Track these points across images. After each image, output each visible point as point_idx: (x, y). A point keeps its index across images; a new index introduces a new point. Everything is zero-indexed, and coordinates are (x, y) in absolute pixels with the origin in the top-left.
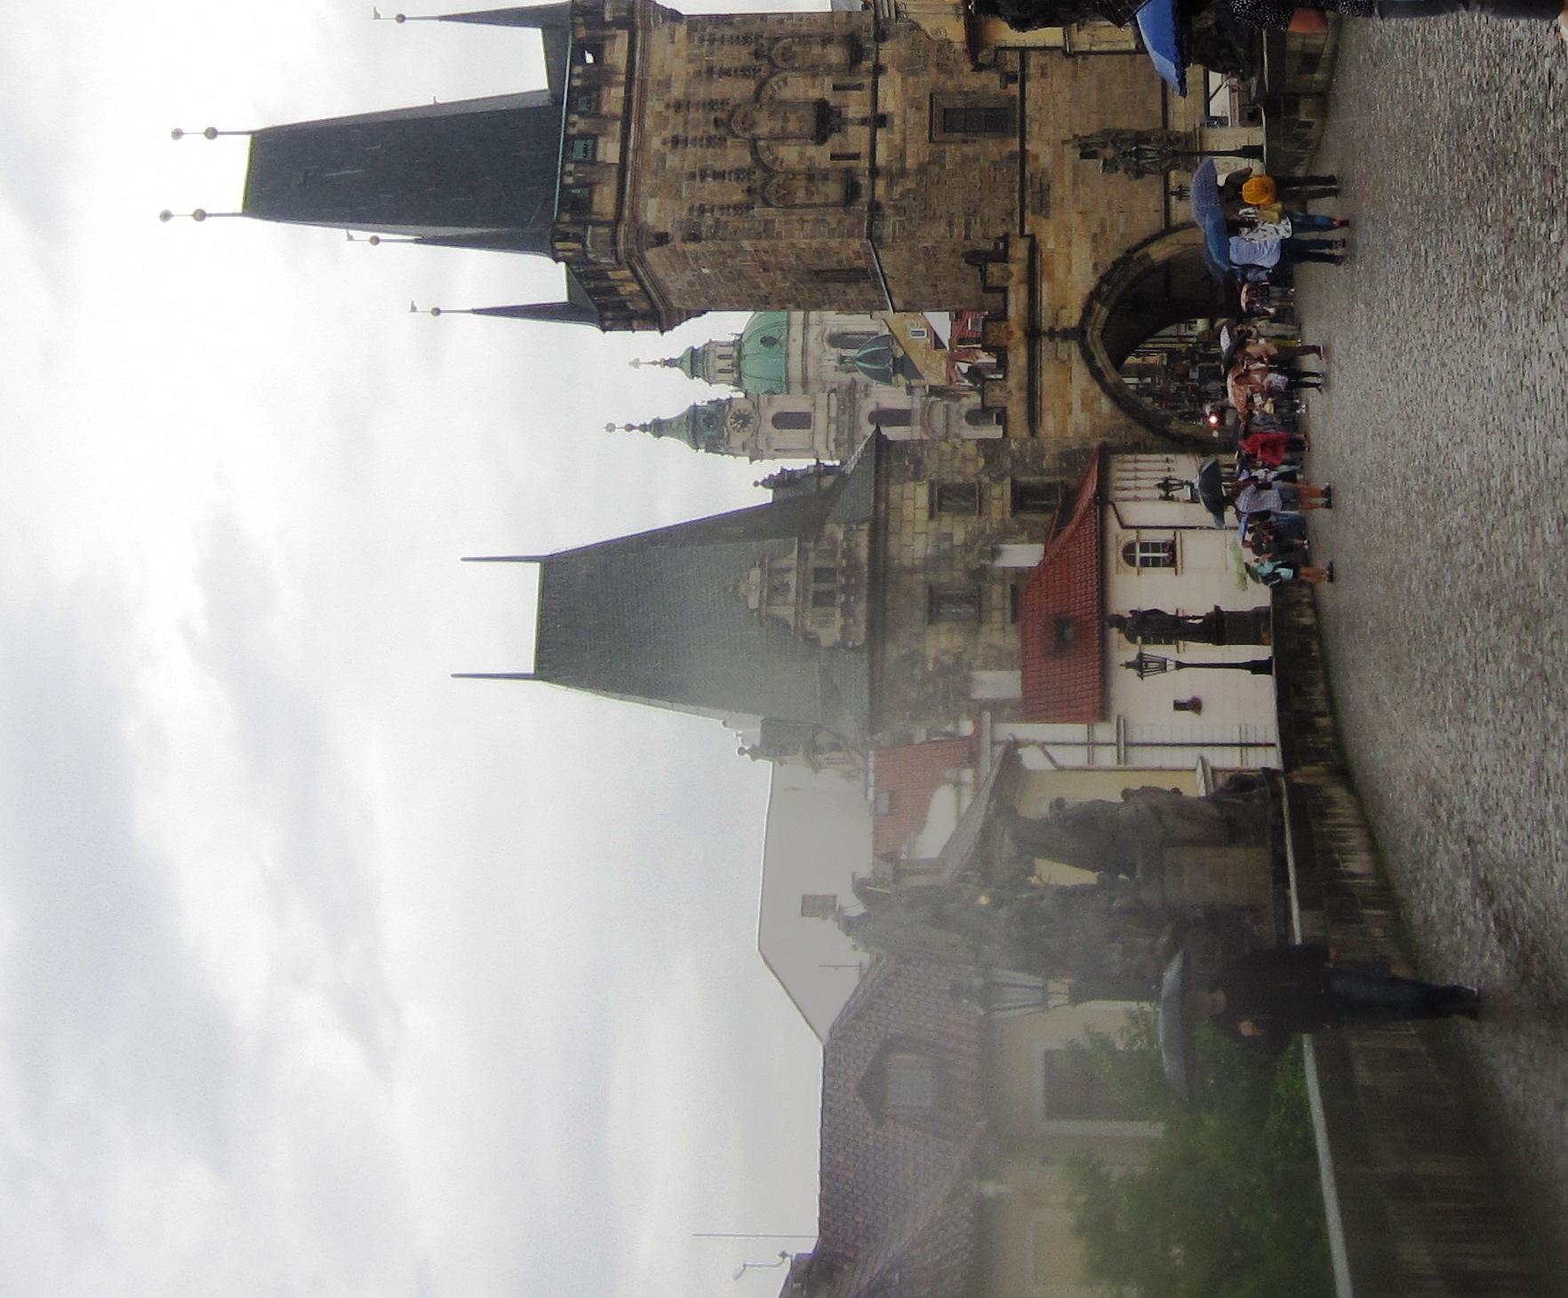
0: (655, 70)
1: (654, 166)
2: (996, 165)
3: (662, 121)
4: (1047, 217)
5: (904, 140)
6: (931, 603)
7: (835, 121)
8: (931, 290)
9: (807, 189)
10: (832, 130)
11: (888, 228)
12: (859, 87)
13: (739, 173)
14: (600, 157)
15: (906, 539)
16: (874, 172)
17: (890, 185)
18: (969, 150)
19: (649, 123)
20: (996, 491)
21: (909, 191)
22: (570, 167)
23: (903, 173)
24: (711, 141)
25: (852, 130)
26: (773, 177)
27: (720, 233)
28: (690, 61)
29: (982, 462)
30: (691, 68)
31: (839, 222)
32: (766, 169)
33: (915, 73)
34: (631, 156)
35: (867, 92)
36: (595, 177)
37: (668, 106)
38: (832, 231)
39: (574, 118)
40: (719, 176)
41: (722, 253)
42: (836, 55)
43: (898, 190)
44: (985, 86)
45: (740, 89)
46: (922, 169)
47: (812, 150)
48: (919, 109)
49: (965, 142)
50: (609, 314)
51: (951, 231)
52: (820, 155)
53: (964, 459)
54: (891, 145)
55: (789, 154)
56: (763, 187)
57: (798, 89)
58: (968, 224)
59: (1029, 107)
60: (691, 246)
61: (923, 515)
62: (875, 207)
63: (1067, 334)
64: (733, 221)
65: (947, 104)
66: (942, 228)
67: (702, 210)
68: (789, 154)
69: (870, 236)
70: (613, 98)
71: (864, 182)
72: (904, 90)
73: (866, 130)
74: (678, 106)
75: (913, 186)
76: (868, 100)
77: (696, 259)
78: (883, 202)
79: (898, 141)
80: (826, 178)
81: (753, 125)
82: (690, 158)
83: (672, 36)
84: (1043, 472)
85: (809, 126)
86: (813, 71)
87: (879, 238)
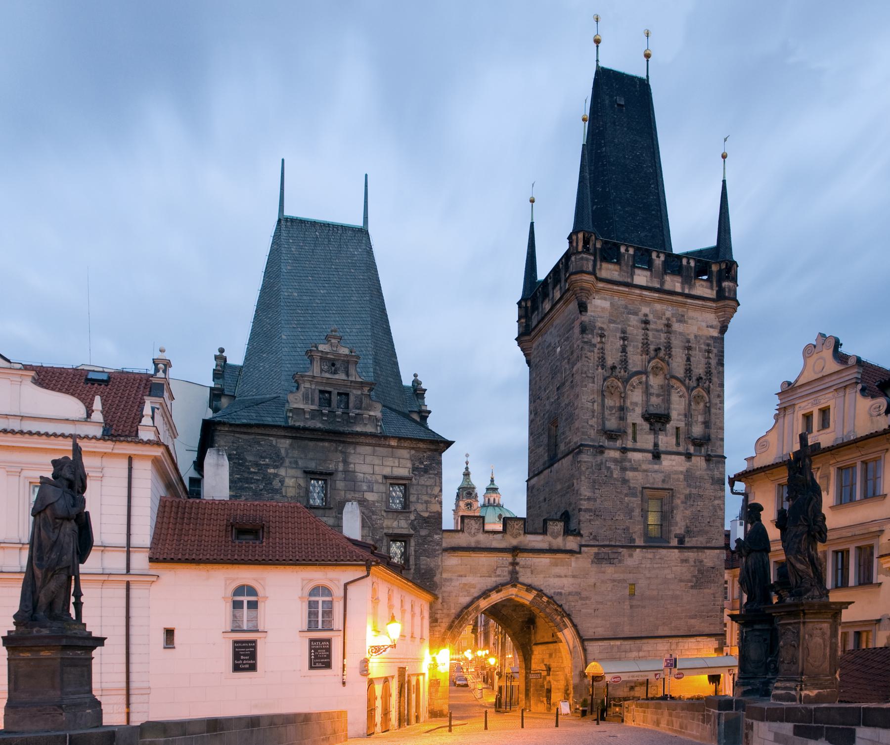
6: (321, 474)
7: (658, 426)
9: (614, 407)
10: (651, 424)
11: (586, 457)
12: (678, 444)
13: (624, 362)
15: (369, 459)
16: (624, 450)
17: (615, 461)
20: (403, 523)
21: (612, 473)
23: (624, 469)
24: (646, 344)
25: (651, 438)
26: (623, 383)
27: (586, 347)
31: (592, 426)
33: (686, 479)
35: (675, 449)
40: (624, 350)
41: (572, 353)
42: (697, 430)
45: (678, 366)
47: (639, 411)
48: (663, 481)
51: (585, 500)
53: (427, 502)
57: (678, 406)
60: (577, 330)
61: (387, 471)
62: (601, 450)
64: (594, 356)
67: (602, 336)
68: (636, 397)
69: (582, 445)
71: (618, 443)
72: (676, 473)
73: (650, 446)
75: (615, 476)
76: (669, 449)
77: (567, 339)
79: (644, 467)
82: (635, 332)
85: (652, 410)
86: (688, 415)
87: (580, 452)
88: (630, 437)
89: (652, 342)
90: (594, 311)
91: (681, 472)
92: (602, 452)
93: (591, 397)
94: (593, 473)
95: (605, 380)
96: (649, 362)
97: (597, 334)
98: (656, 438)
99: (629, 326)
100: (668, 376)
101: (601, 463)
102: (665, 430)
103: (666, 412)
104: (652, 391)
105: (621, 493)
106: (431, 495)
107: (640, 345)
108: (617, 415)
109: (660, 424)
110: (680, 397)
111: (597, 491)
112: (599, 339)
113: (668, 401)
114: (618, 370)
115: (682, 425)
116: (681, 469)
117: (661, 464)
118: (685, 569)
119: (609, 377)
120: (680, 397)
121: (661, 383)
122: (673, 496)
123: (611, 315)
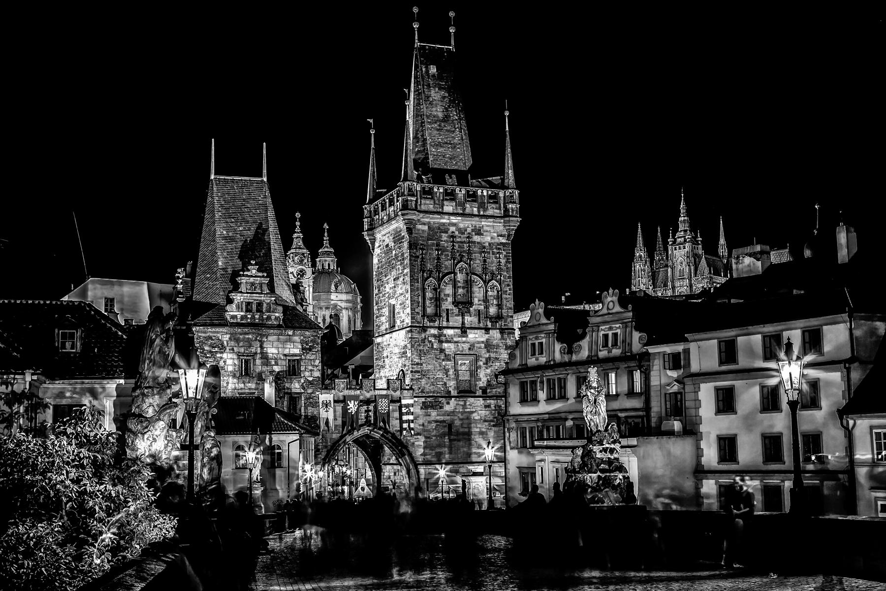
3: (462, 231)
4: (422, 408)
8: (385, 355)
17: (434, 336)
20: (297, 385)
23: (441, 342)
28: (490, 244)
29: (311, 379)
34: (447, 217)
42: (493, 310)
44: (480, 379)
46: (442, 351)
47: (450, 299)
48: (470, 349)
50: (372, 209)
52: (448, 304)
53: (311, 370)
54: (452, 337)
55: (449, 290)
58: (418, 372)
62: (424, 329)
63: (367, 417)
71: (436, 324)
72: (479, 343)
78: (428, 333)
79: (455, 339)
83: (501, 236)
84: (306, 408)
86: (486, 300)
87: (411, 331)
88: (445, 319)
91: (483, 342)
92: (425, 331)
94: (419, 345)
98: (463, 318)
102: (469, 312)
104: (459, 285)
106: (314, 366)
115: (482, 307)
116: (482, 340)
117: (467, 336)
118: (488, 413)
123: (429, 234)
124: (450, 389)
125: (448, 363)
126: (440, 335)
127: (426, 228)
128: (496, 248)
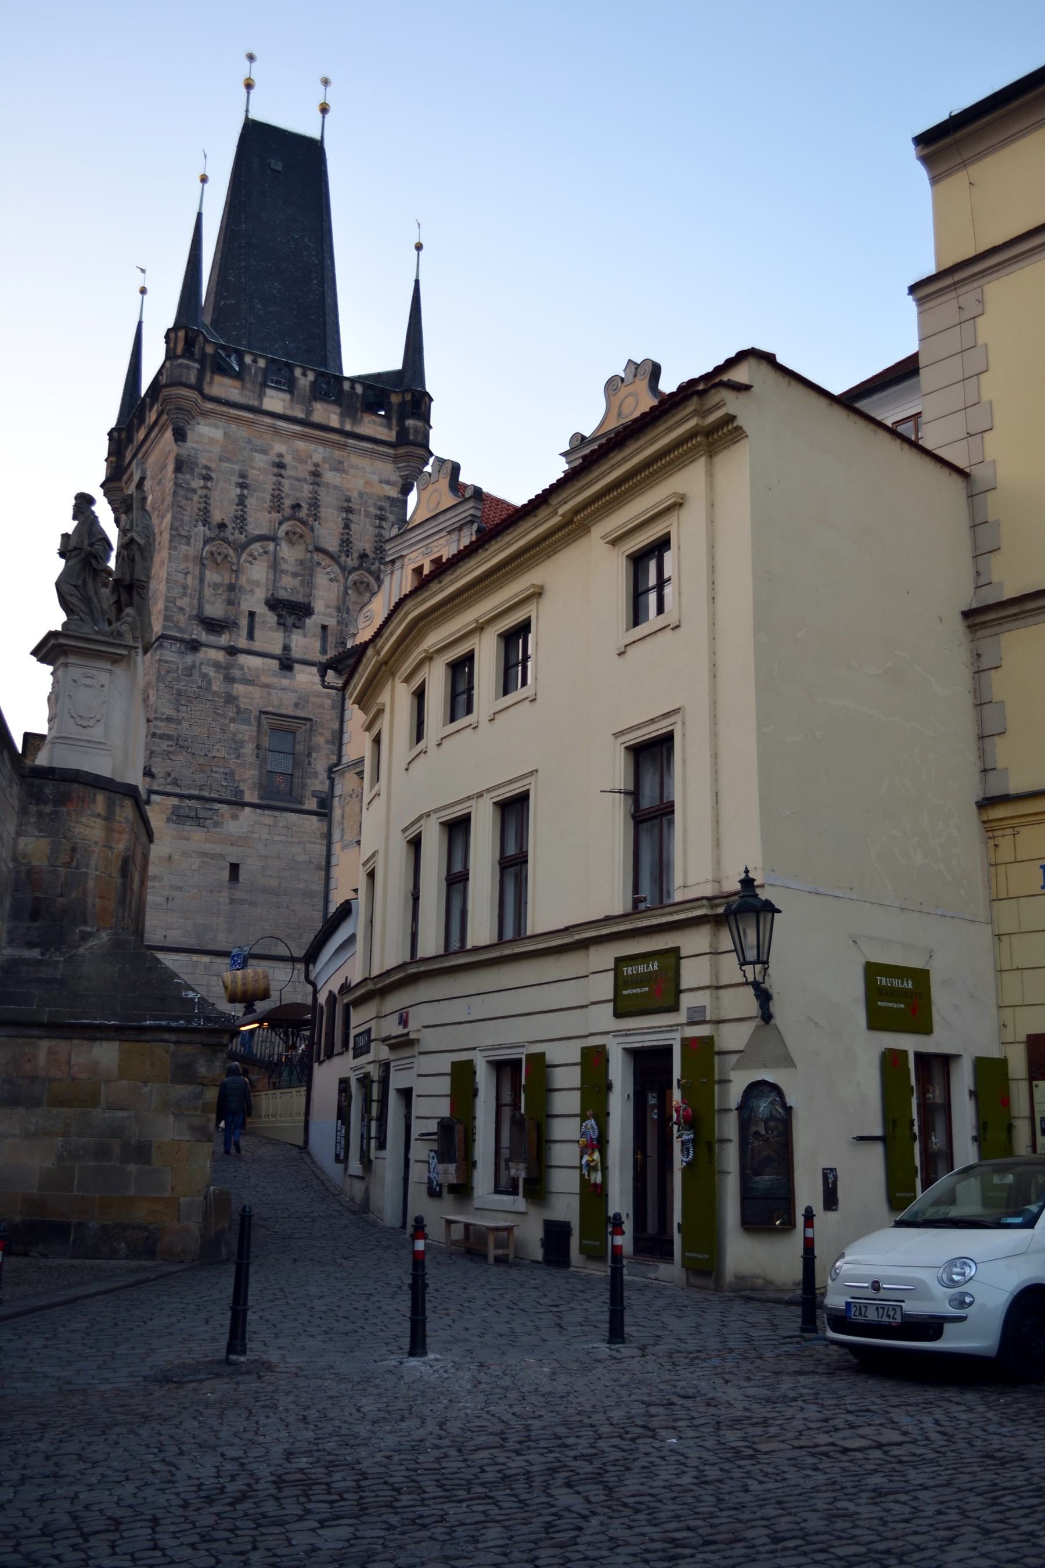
0: (355, 460)
1: (257, 441)
2: (230, 775)
4: (169, 820)
5: (266, 686)
7: (290, 620)
9: (222, 585)
10: (279, 616)
12: (324, 651)
13: (241, 520)
14: (268, 391)
17: (217, 665)
18: (249, 749)
19: (301, 445)
21: (209, 682)
22: (262, 363)
23: (229, 679)
24: (277, 498)
26: (235, 550)
27: (182, 492)
28: (361, 494)
30: (354, 495)
31: (181, 609)
32: (244, 546)
34: (268, 420)
36: (249, 385)
37: (317, 465)
38: (168, 599)
39: (311, 376)
40: (241, 501)
43: (212, 673)
44: (316, 775)
46: (231, 699)
47: (260, 594)
48: (296, 705)
49: (258, 747)
50: (124, 435)
51: (162, 720)
52: (254, 601)
55: (257, 572)
56: (225, 540)
57: (325, 595)
58: (169, 737)
59: (293, 817)
60: (171, 467)
62: (194, 646)
64: (193, 506)
65: (299, 736)
66: (169, 712)
67: (207, 478)
68: (257, 572)
69: (163, 637)
70: (328, 414)
71: (224, 640)
73: (278, 650)
74: (316, 474)
75: (215, 688)
76: (309, 657)
79: (264, 679)
80: (230, 602)
81: (291, 542)
83: (388, 482)
87: (161, 646)
88: (244, 632)
89: (288, 495)
90: (197, 442)
93: (183, 566)
94: (178, 679)
95: (206, 542)
96: (281, 523)
97: (200, 474)
99: (253, 468)
100: (311, 548)
101: (193, 667)
103: (306, 600)
104: (284, 566)
105: (223, 715)
107: (269, 498)
108: (225, 596)
109: (293, 617)
110: (331, 580)
111: (182, 708)
112: (202, 483)
113: (309, 585)
114: (230, 529)
117: (293, 678)
119: (213, 539)
120: (331, 580)
121: (301, 557)
122: (311, 730)
124: (243, 786)
125: (247, 728)
126: (228, 667)
127: (218, 434)
128: (375, 505)
